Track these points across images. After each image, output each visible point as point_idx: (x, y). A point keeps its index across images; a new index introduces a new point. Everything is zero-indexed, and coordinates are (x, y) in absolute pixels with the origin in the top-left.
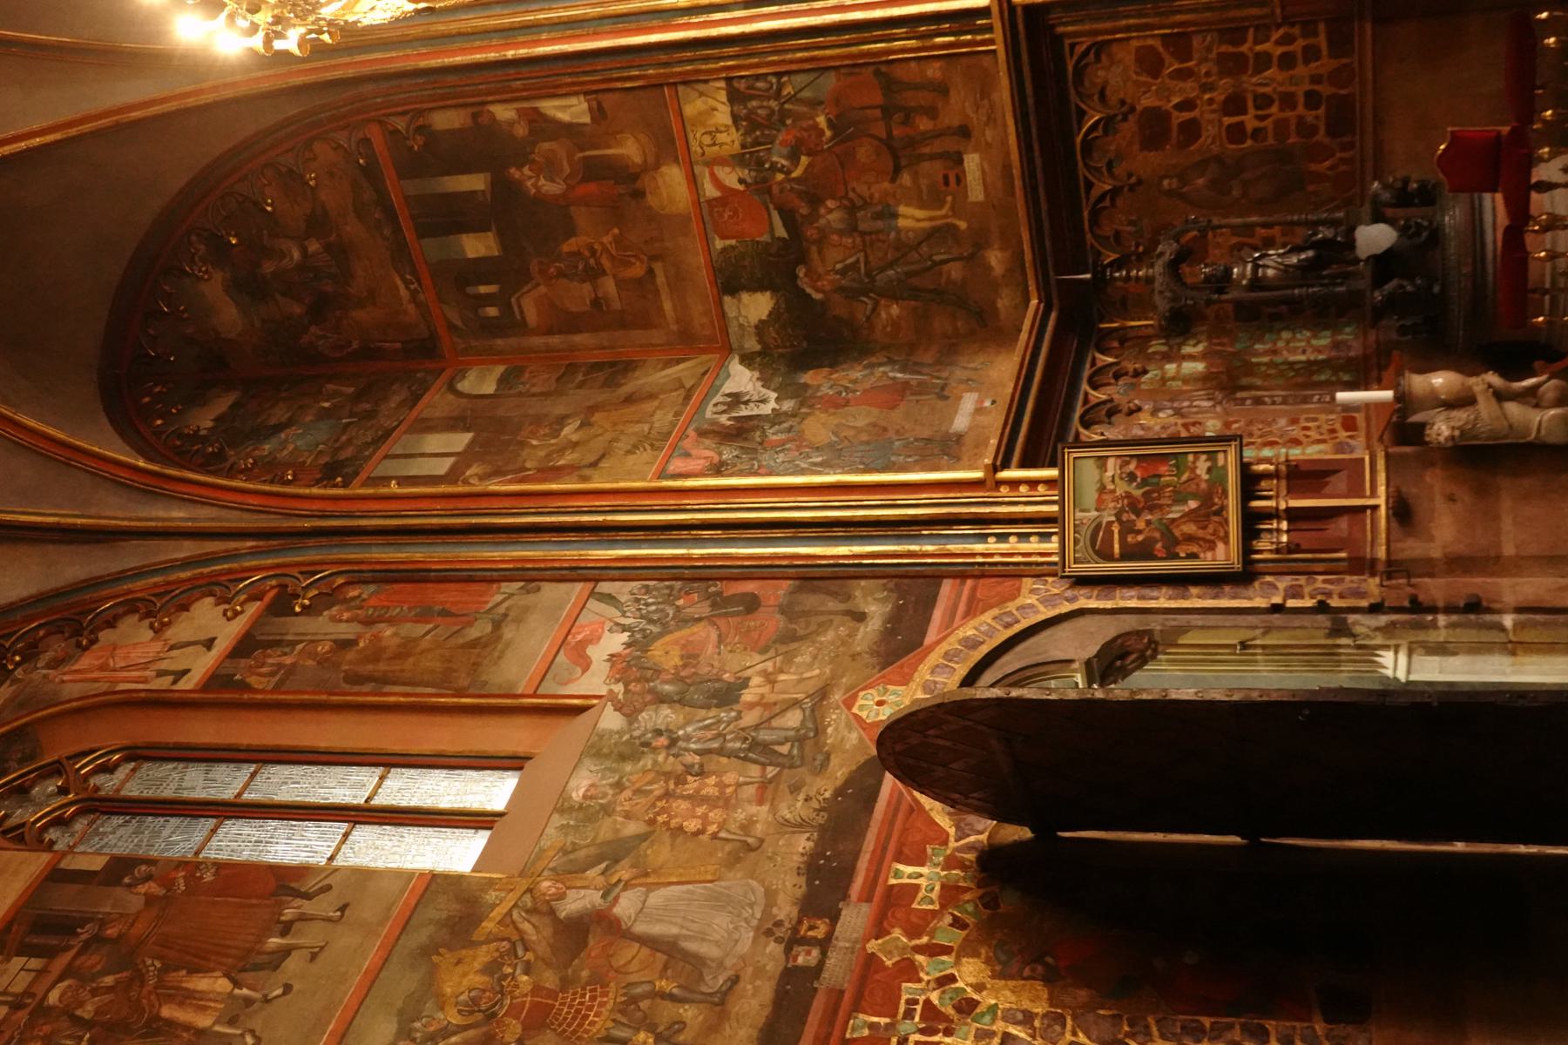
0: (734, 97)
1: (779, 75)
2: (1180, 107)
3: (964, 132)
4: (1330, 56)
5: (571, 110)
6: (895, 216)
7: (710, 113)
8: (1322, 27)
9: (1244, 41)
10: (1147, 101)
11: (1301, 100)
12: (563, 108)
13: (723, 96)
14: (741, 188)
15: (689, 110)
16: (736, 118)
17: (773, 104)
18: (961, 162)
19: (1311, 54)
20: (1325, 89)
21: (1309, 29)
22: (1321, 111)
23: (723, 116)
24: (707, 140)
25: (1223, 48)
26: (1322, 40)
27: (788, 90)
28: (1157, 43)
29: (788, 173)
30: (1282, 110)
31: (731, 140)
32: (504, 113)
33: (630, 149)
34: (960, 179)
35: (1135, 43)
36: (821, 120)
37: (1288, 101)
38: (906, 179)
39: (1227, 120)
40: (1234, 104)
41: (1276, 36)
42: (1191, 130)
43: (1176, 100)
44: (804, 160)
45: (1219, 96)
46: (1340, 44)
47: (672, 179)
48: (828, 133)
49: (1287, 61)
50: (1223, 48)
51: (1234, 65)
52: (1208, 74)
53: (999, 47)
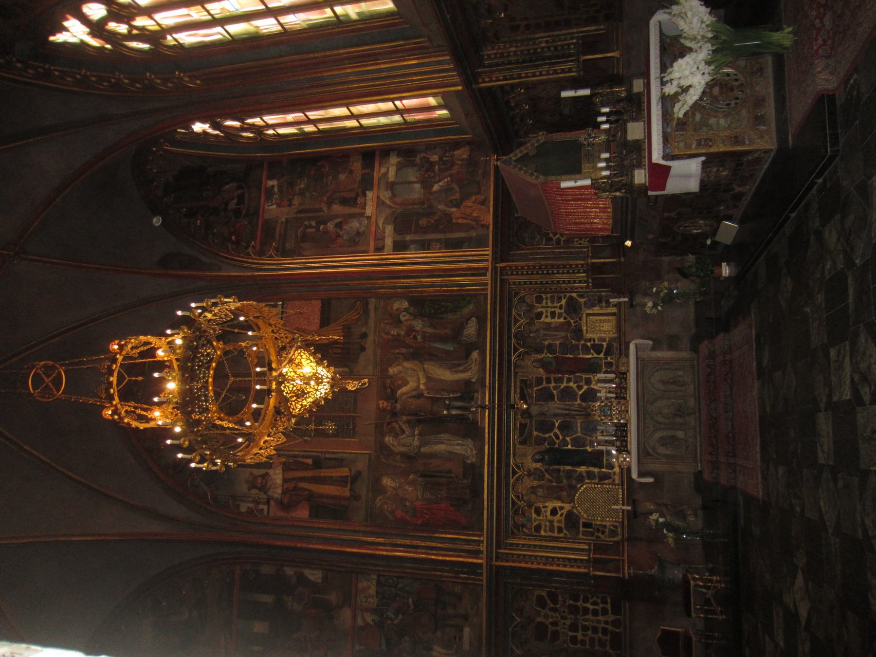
0: (379, 583)
1: (398, 578)
2: (551, 623)
3: (466, 617)
4: (613, 613)
5: (314, 575)
6: (431, 649)
7: (369, 587)
8: (609, 600)
9: (579, 601)
10: (539, 619)
11: (600, 630)
12: (312, 575)
13: (374, 583)
14: (372, 623)
15: (360, 586)
16: (377, 593)
17: (393, 590)
18: (462, 630)
19: (605, 612)
20: (610, 628)
21: (604, 602)
22: (608, 637)
23: (373, 591)
24: (364, 600)
25: (571, 602)
26: (609, 606)
27: (400, 585)
28: (544, 594)
29: (393, 621)
30: (593, 633)
31: (373, 602)
32: (289, 571)
33: (333, 598)
34: (461, 639)
35: (536, 593)
36: (410, 600)
37: (595, 630)
38: (439, 634)
39: (571, 634)
40: (574, 627)
41: (591, 601)
42: (556, 634)
43: (551, 620)
44: (400, 616)
45: (568, 622)
46: (616, 610)
47: (347, 613)
48: (412, 607)
49: (595, 613)
50: (571, 602)
51: (574, 610)
52: (564, 612)
53: (484, 583)
